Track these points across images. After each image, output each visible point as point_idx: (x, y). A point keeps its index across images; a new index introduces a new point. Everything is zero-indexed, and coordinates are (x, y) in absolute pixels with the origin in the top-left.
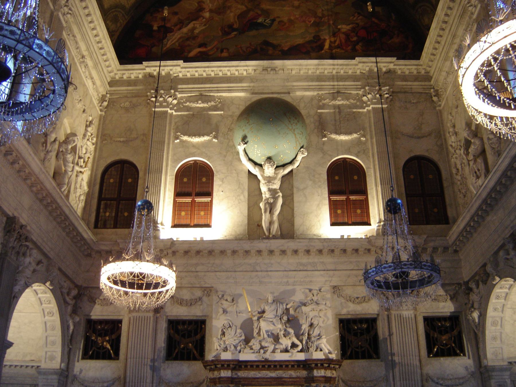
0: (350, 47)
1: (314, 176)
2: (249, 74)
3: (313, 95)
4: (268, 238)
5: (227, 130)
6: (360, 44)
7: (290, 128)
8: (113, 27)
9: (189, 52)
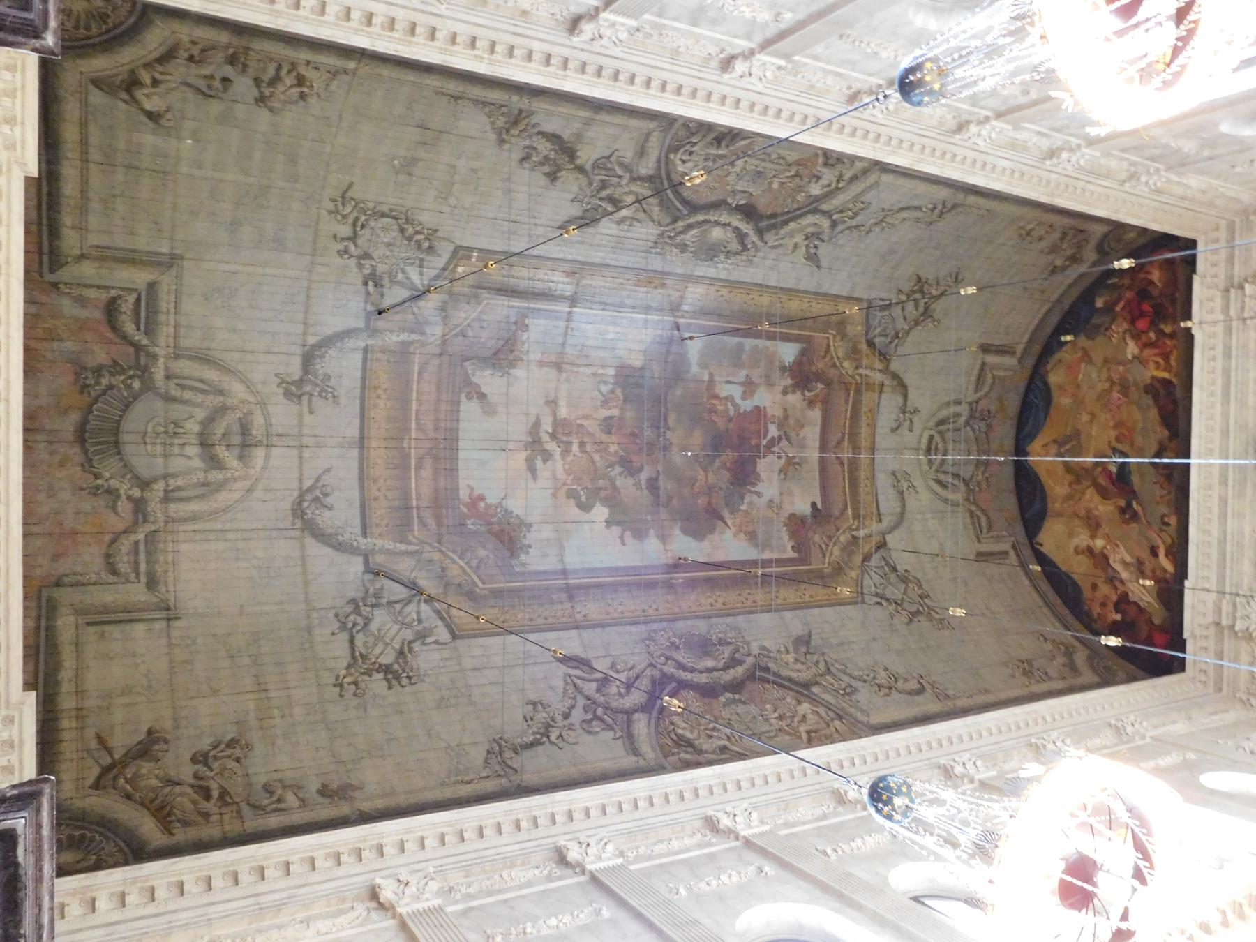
0: (1168, 342)
6: (1162, 326)
8: (1121, 675)
9: (1165, 571)
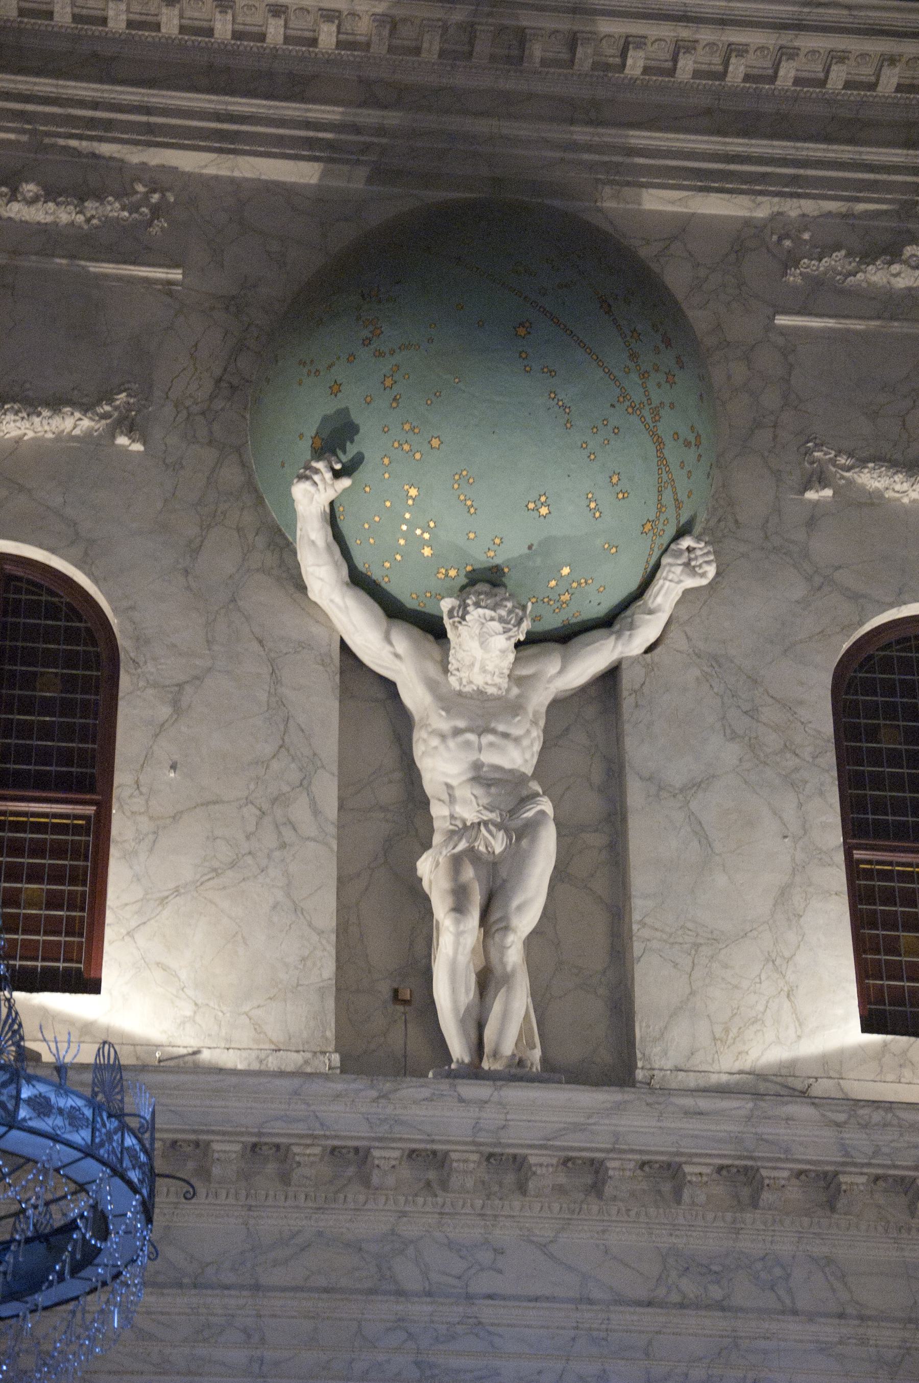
1: (752, 713)
2: (351, 45)
3: (747, 222)
4: (474, 1071)
5: (209, 386)
7: (637, 396)
